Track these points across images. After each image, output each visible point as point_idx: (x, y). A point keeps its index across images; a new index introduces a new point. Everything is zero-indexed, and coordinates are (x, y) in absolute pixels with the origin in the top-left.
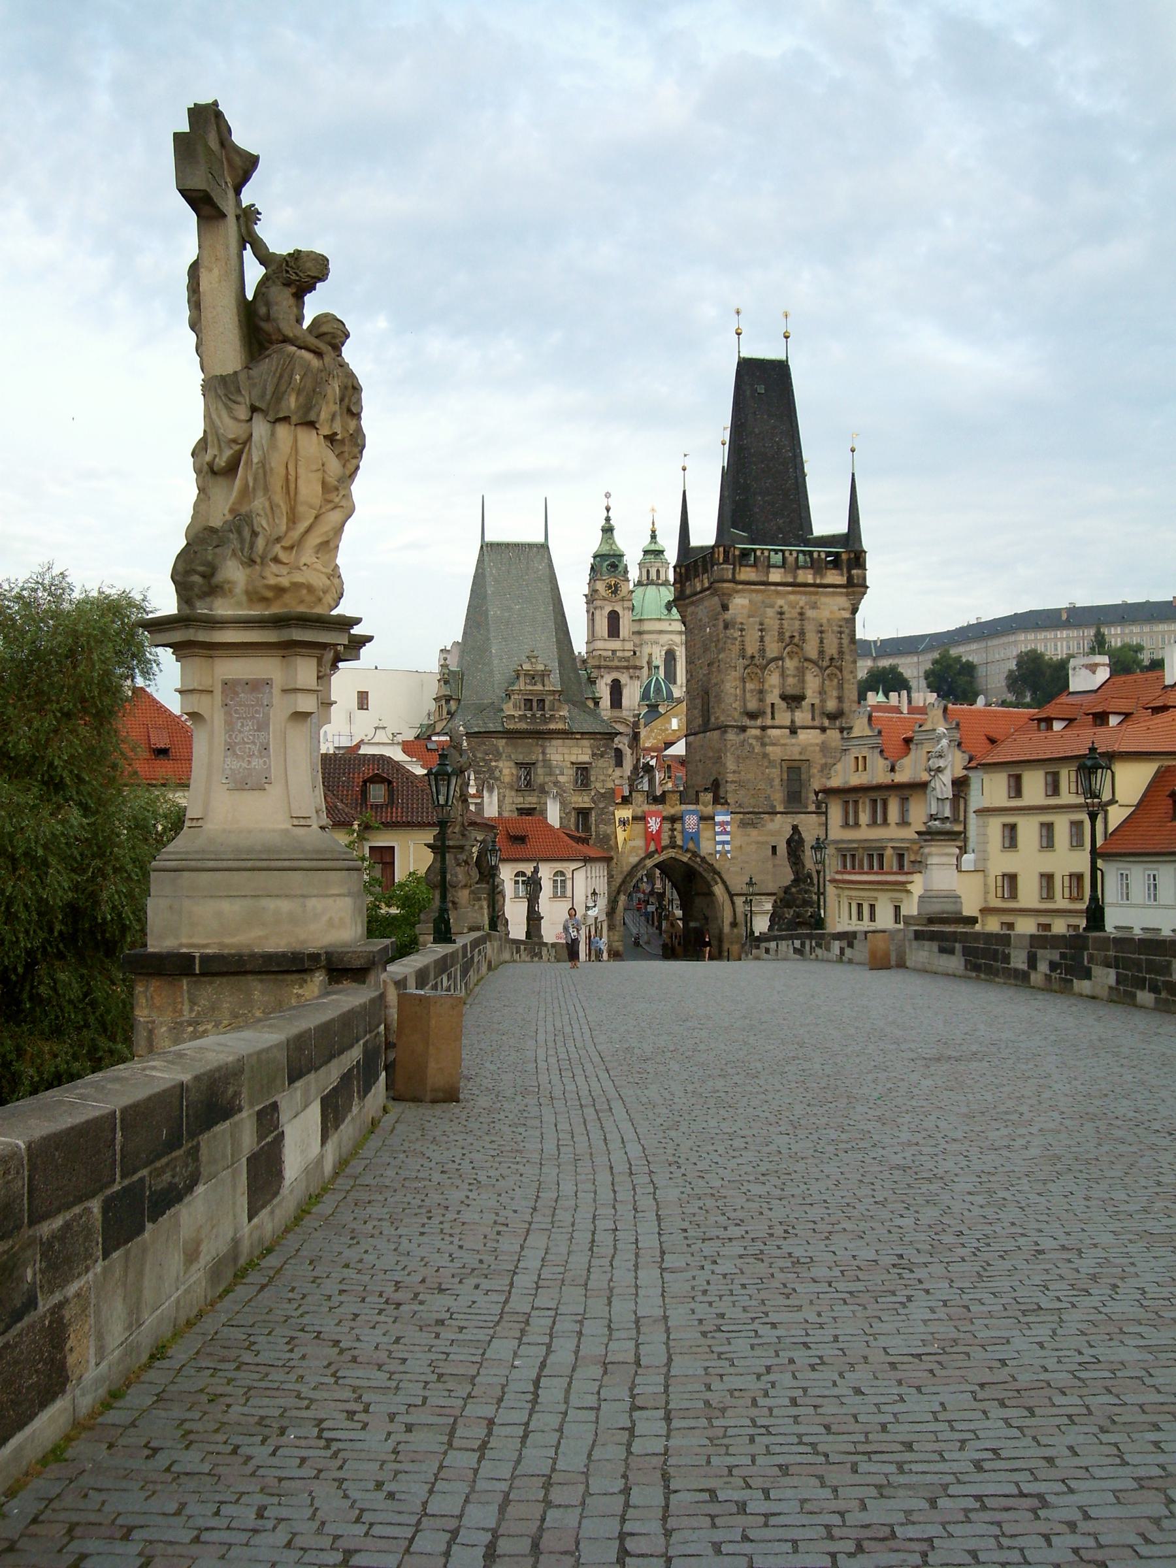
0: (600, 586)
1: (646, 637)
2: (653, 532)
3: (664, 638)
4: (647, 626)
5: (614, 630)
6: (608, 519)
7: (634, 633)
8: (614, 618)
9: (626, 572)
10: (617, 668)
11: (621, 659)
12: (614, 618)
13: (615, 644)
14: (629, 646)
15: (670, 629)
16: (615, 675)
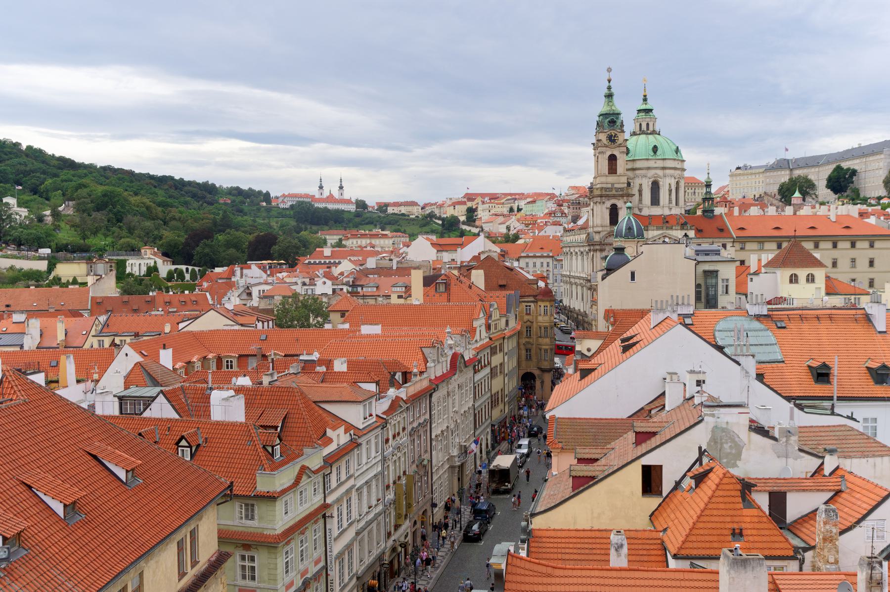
0: (603, 137)
1: (638, 172)
2: (645, 96)
3: (651, 173)
4: (638, 165)
5: (612, 170)
6: (609, 88)
7: (628, 170)
8: (612, 159)
9: (622, 125)
10: (614, 196)
11: (617, 189)
12: (612, 159)
13: (612, 179)
14: (624, 180)
15: (656, 165)
16: (613, 201)
